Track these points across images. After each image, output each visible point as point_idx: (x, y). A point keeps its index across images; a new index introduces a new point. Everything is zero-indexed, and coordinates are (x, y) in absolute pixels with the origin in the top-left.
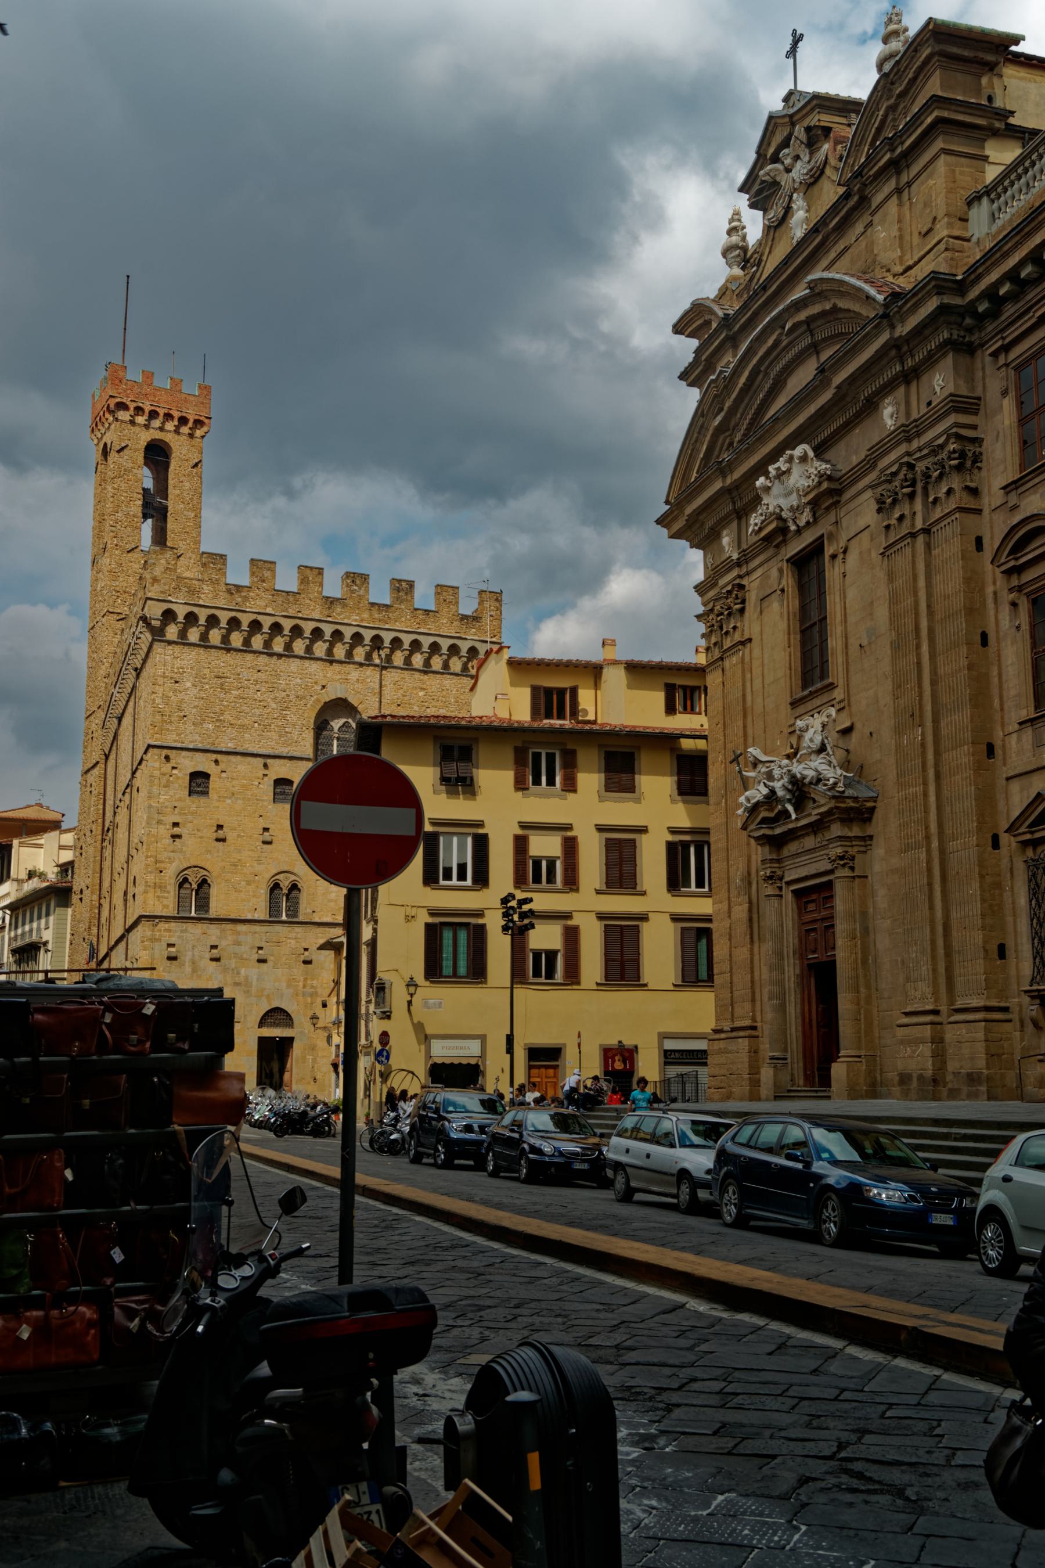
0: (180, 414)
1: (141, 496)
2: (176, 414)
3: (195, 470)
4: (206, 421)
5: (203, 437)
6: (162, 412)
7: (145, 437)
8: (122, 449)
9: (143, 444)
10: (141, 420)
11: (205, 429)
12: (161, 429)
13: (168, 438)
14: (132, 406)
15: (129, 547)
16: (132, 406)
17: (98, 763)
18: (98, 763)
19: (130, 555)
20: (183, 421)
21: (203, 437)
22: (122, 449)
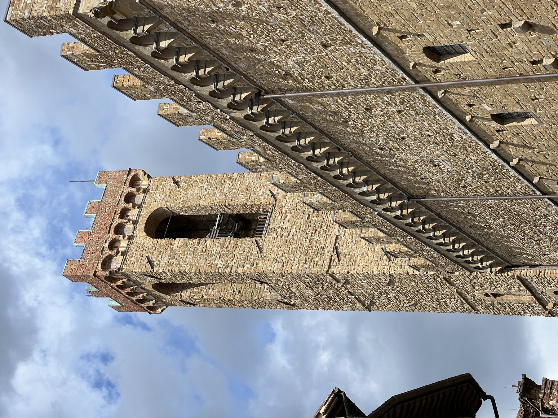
0: (123, 202)
1: (202, 240)
2: (122, 205)
3: (182, 184)
4: (132, 174)
5: (149, 177)
6: (118, 221)
7: (141, 237)
8: (150, 262)
9: (150, 241)
10: (123, 244)
11: (141, 175)
12: (135, 222)
13: (146, 213)
14: (108, 252)
15: (256, 250)
16: (108, 252)
17: (519, 278)
18: (519, 278)
19: (265, 250)
20: (129, 198)
21: (149, 177)
22: (150, 262)
